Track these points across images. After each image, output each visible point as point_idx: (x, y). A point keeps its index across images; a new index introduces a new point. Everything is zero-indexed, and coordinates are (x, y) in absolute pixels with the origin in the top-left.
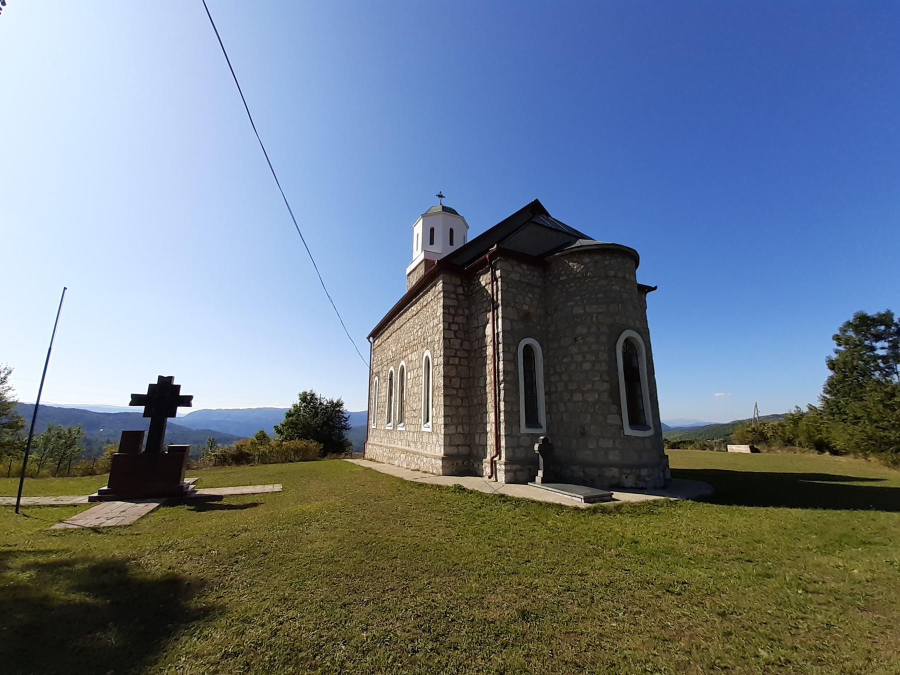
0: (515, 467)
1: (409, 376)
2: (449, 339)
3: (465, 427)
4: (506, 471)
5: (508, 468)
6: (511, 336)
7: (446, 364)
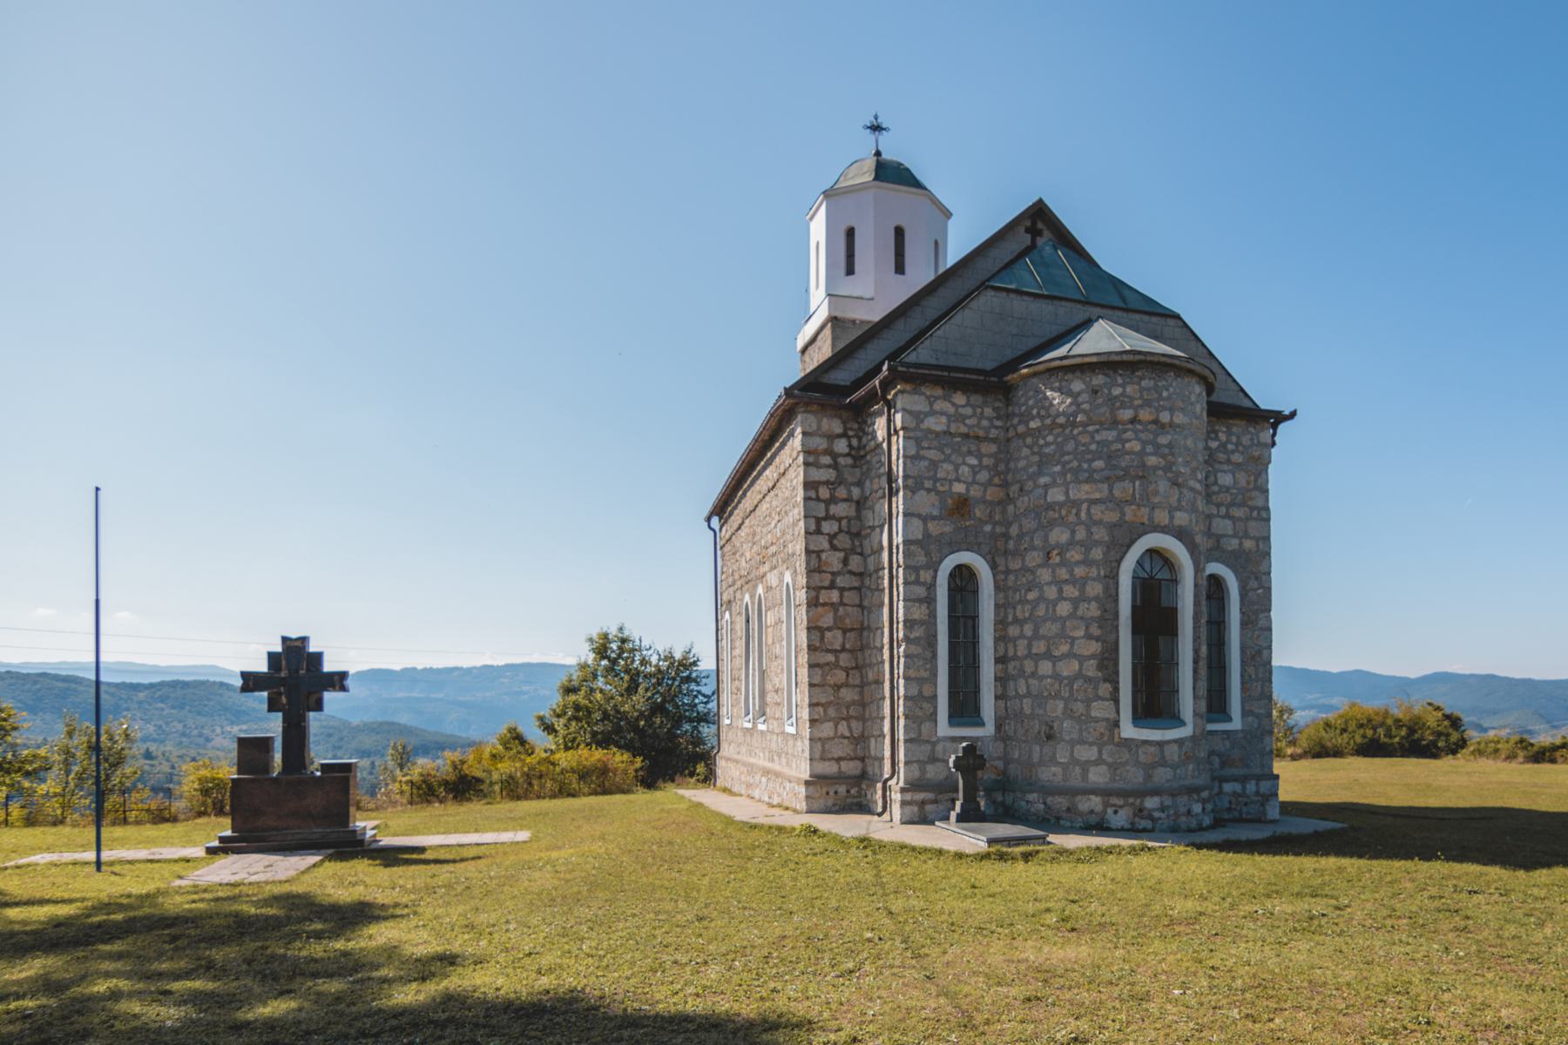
0: (920, 796)
1: (770, 618)
2: (818, 553)
3: (854, 724)
4: (904, 803)
5: (908, 797)
6: (924, 550)
7: (813, 603)
